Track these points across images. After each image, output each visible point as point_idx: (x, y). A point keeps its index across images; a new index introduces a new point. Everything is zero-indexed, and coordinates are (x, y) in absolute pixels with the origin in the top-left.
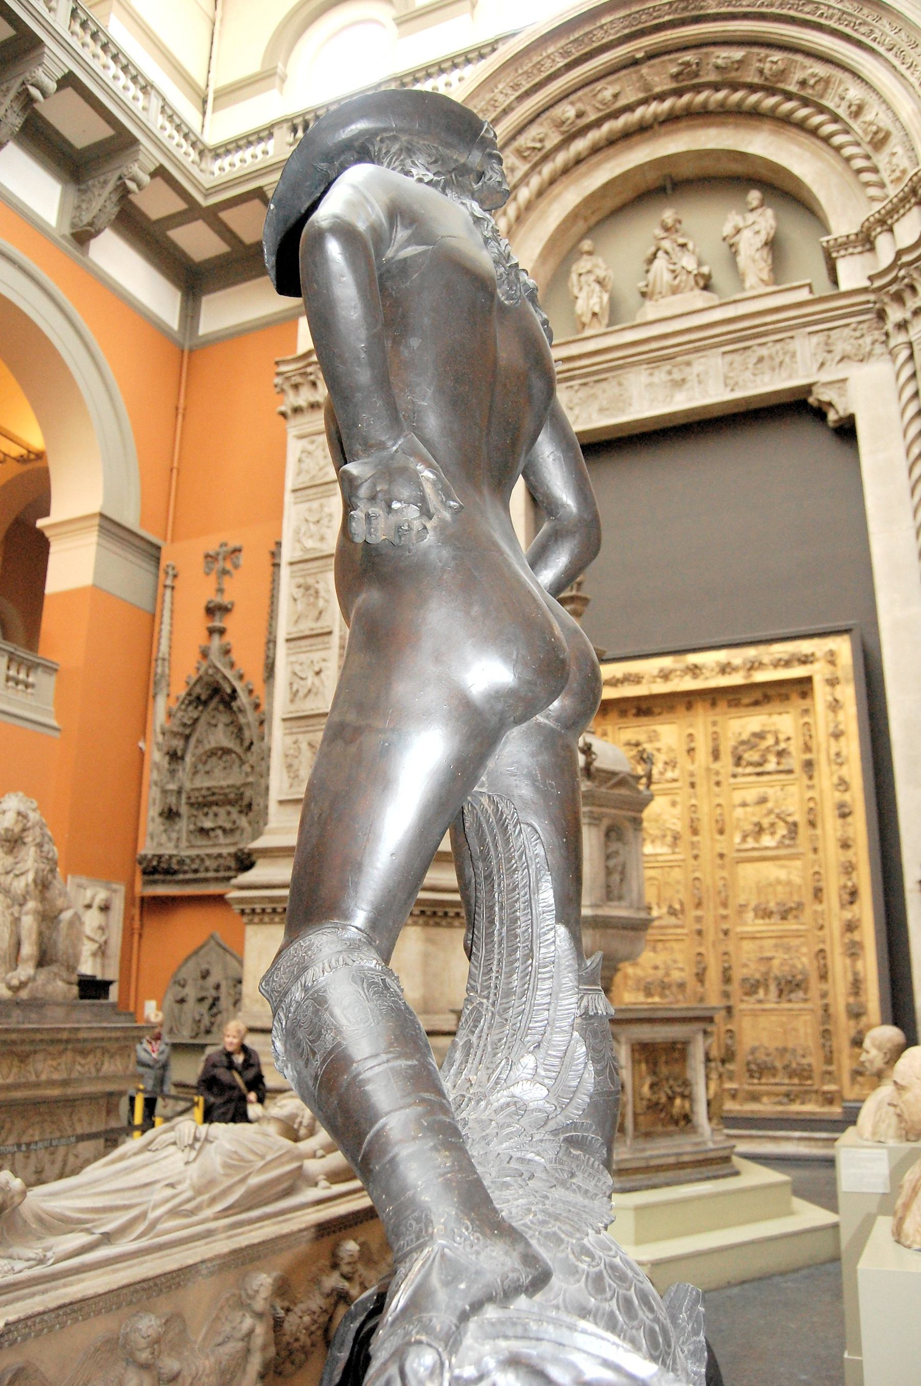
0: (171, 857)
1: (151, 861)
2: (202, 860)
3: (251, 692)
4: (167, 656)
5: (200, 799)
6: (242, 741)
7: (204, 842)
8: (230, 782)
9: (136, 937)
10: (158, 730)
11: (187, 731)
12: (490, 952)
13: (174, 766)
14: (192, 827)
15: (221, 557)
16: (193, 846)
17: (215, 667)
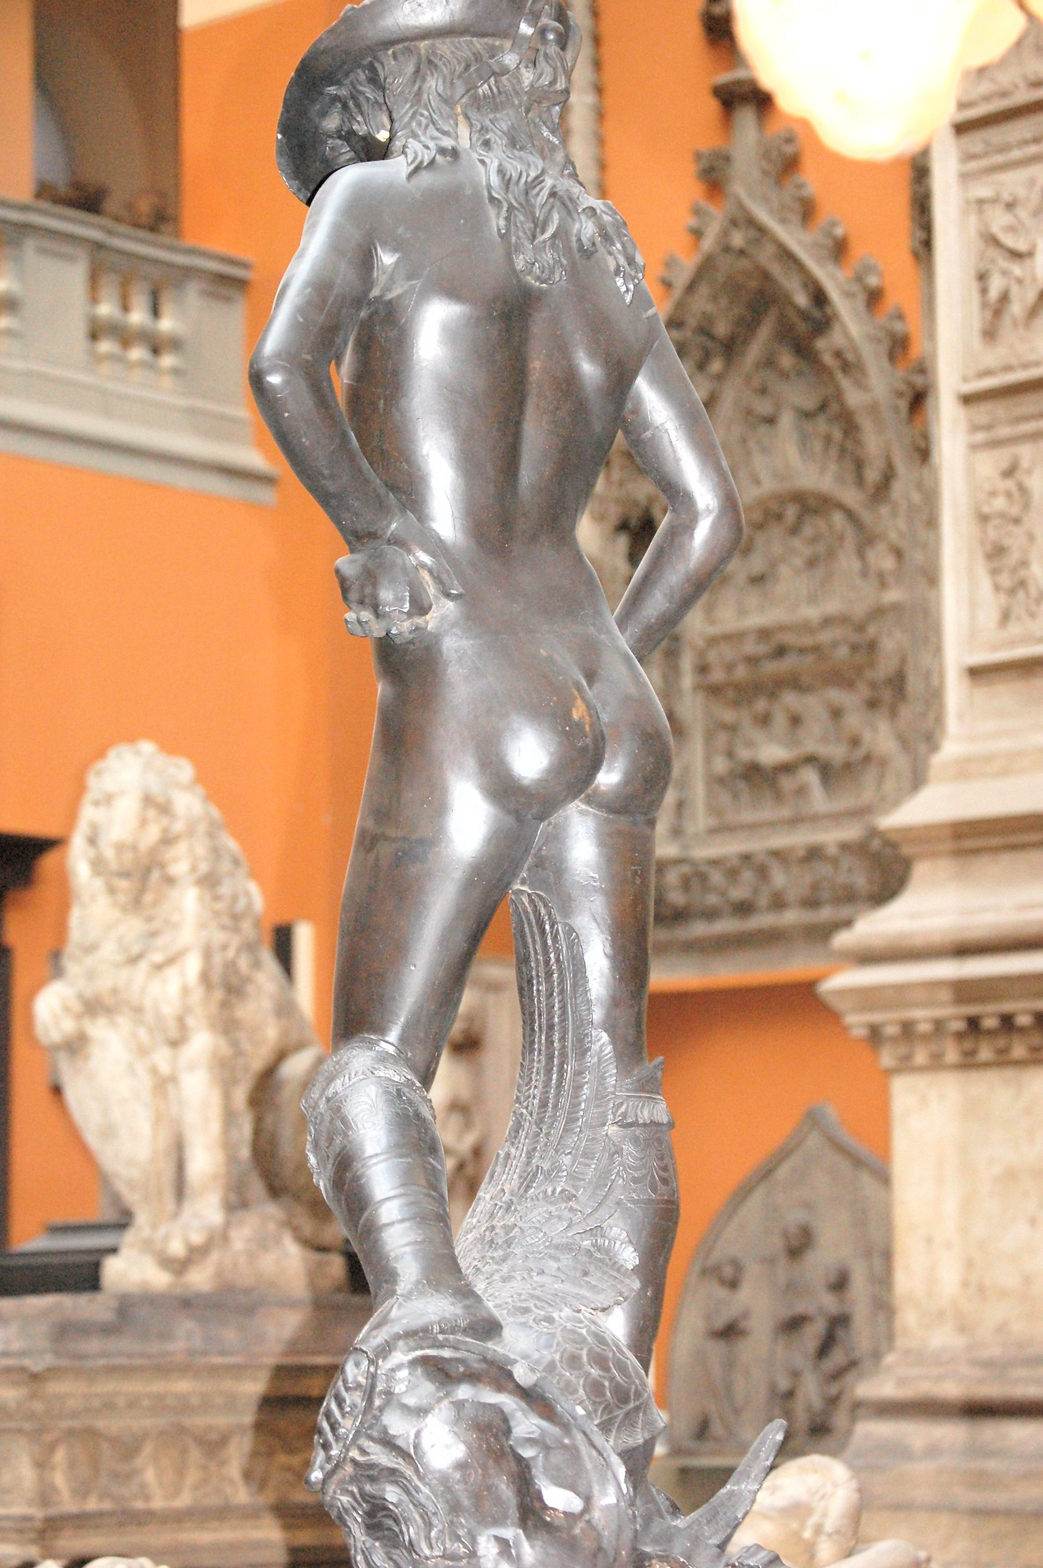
2: (762, 872)
3: (874, 298)
5: (741, 672)
6: (859, 465)
7: (767, 813)
8: (832, 606)
14: (721, 765)
16: (722, 829)
17: (752, 223)
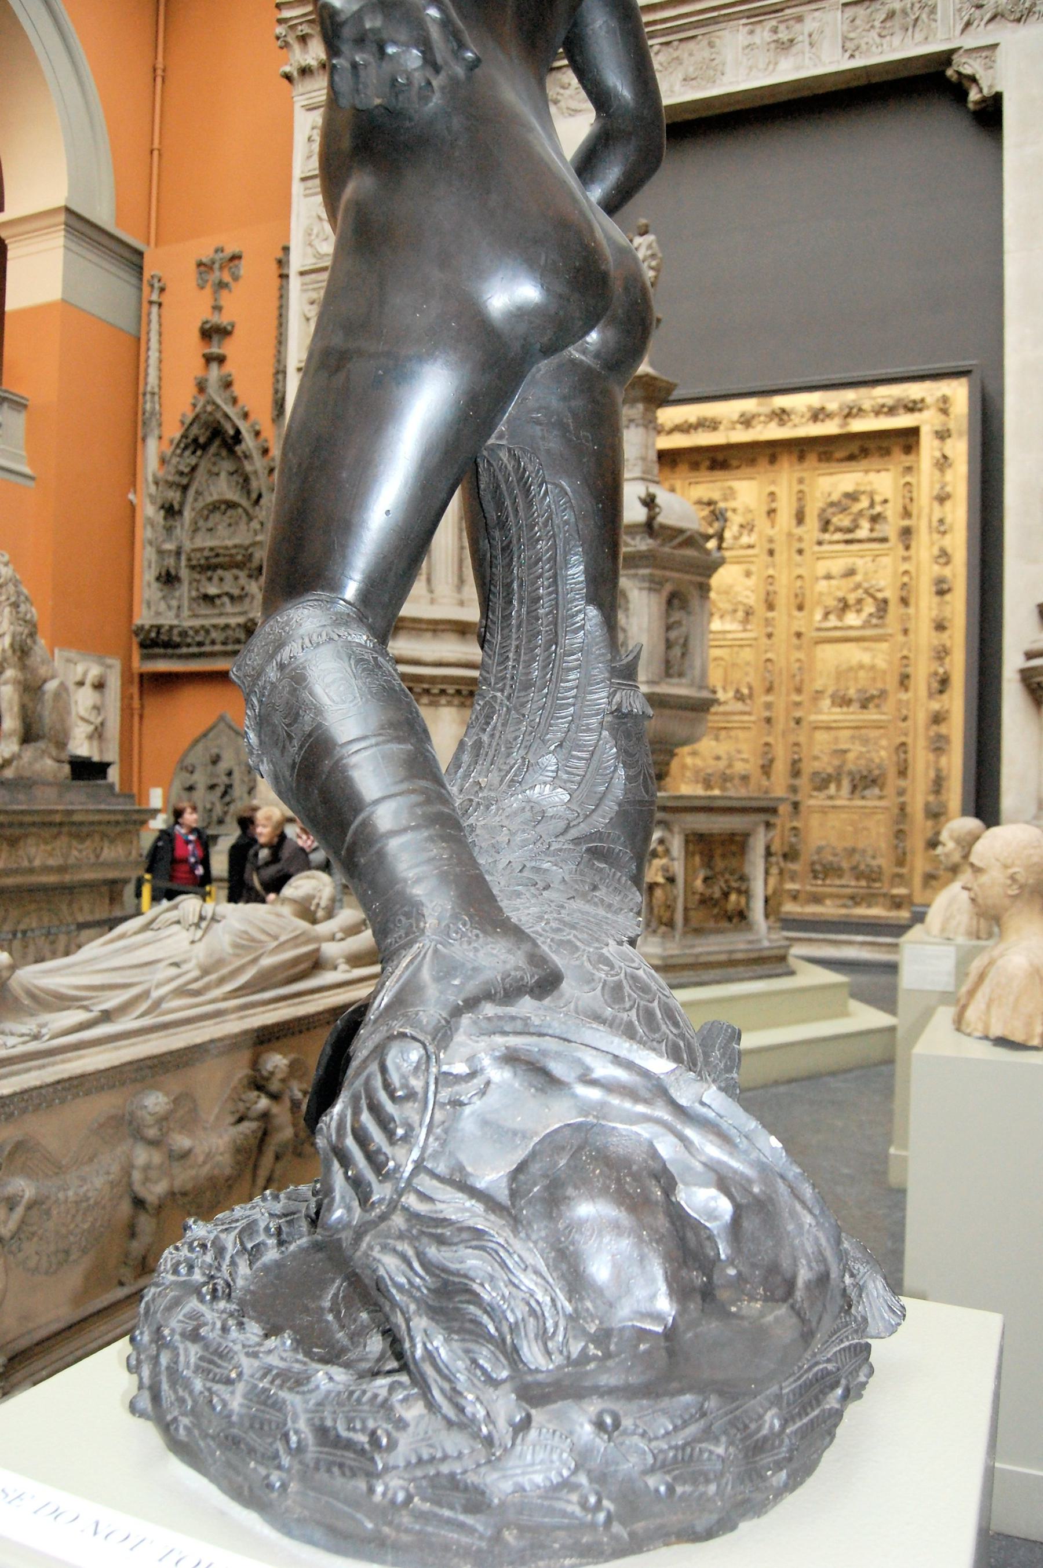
0: (171, 627)
1: (149, 631)
2: (207, 632)
3: (257, 434)
4: (156, 390)
5: (202, 562)
6: (249, 493)
7: (208, 612)
8: (237, 541)
9: (136, 718)
10: (150, 479)
11: (184, 481)
12: (506, 638)
13: (170, 522)
14: (194, 594)
15: (217, 266)
17: (214, 403)
